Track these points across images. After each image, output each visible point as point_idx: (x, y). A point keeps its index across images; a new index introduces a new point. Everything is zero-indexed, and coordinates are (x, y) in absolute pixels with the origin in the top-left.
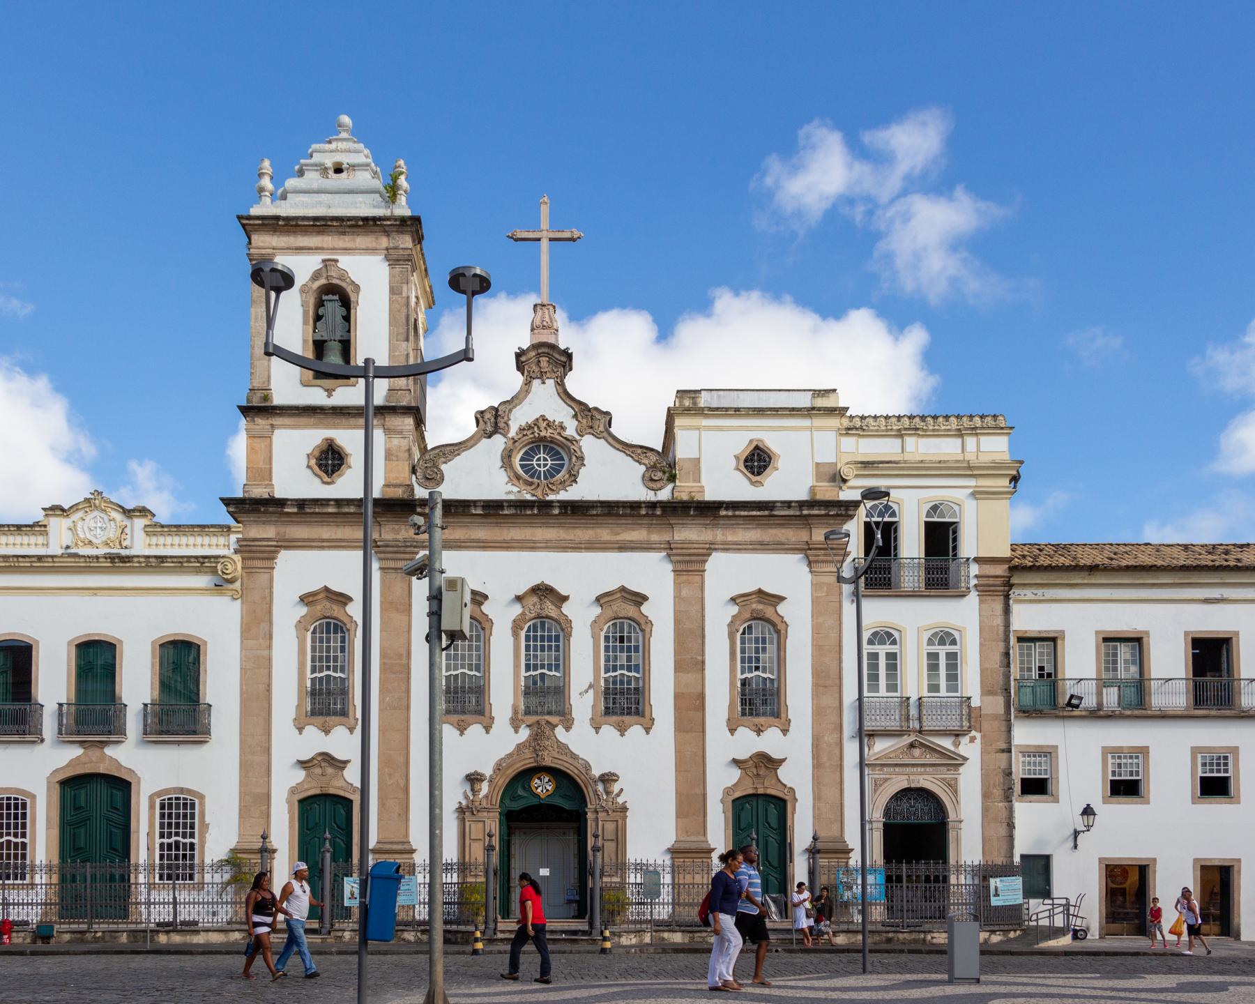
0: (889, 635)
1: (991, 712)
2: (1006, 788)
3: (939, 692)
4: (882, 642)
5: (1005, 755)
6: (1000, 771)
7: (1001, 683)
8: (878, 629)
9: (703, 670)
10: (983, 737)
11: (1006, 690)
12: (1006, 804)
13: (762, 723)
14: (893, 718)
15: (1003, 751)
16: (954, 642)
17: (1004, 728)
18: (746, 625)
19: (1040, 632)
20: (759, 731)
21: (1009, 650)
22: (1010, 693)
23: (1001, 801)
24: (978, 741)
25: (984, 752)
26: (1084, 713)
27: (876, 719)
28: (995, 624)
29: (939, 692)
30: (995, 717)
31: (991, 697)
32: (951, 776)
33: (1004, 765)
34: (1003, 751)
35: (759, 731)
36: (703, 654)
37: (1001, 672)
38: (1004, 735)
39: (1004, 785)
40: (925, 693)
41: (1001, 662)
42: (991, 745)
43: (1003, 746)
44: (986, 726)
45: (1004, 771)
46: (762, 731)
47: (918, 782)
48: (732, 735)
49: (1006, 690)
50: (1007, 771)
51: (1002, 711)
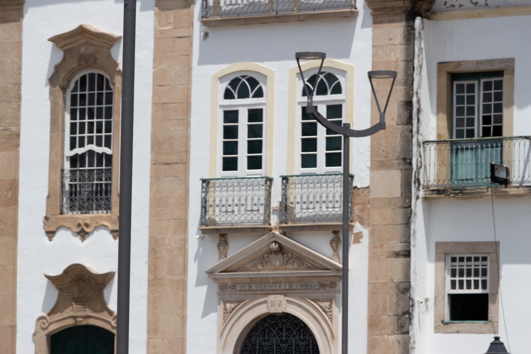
0: (253, 82)
1: (384, 195)
2: (400, 311)
3: (315, 166)
4: (243, 94)
5: (401, 261)
6: (393, 285)
7: (399, 149)
8: (238, 75)
9: (18, 145)
10: (372, 233)
11: (405, 159)
12: (400, 337)
13: (88, 222)
14: (243, 208)
15: (397, 255)
16: (338, 90)
17: (400, 220)
18: (78, 77)
19: (478, 62)
20: (83, 234)
21: (412, 97)
22: (411, 164)
23: (393, 333)
24: (365, 240)
25: (373, 256)
26: (521, 191)
27: (233, 212)
28: (393, 59)
29: (315, 166)
30: (389, 202)
31: (383, 172)
32: (325, 294)
33: (398, 277)
34: (397, 255)
35: (83, 234)
36: (18, 125)
37: (399, 132)
38: (400, 230)
39: (397, 306)
40: (298, 169)
41: (399, 116)
42: (381, 246)
43: (399, 247)
44: (376, 217)
45: (397, 286)
46: (87, 233)
47: (280, 305)
48: (50, 240)
49: (405, 159)
50: (402, 286)
51: (397, 192)
